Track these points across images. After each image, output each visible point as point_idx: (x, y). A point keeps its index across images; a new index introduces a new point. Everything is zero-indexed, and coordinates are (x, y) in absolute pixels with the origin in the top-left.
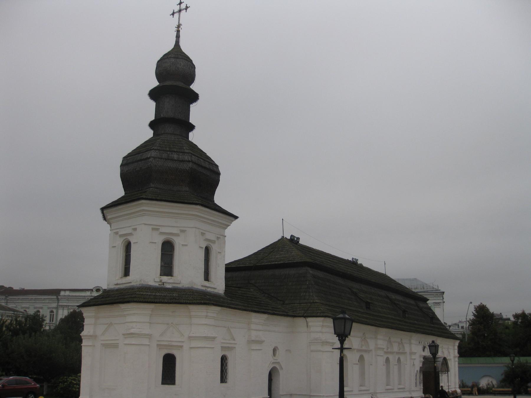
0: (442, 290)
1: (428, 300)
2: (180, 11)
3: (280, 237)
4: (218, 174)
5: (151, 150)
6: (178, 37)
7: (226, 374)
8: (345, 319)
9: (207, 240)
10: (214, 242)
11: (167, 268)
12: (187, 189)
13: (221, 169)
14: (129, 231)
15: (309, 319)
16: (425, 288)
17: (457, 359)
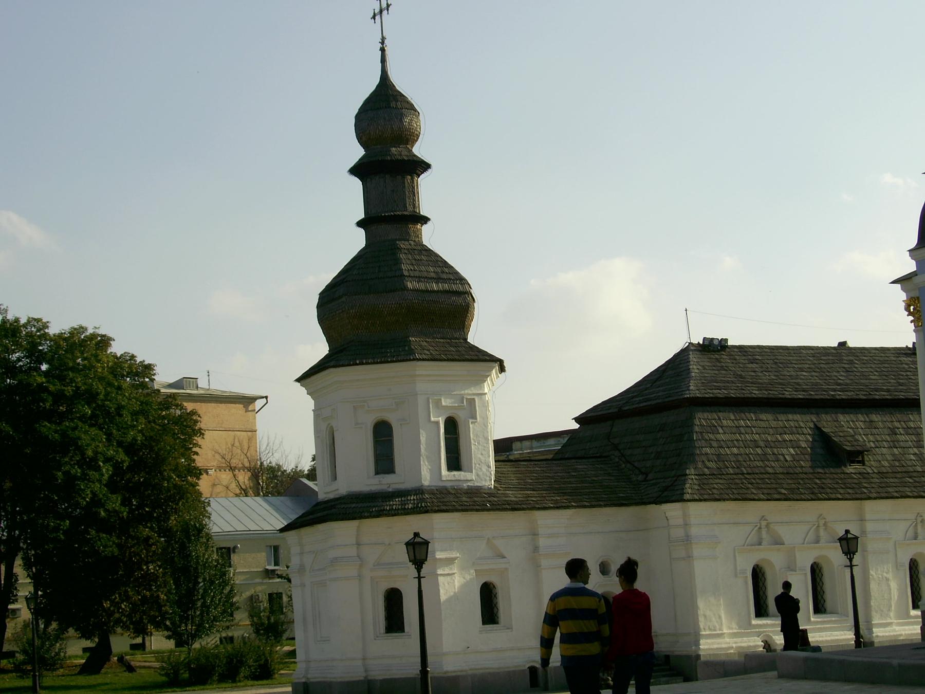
2: (381, 11)
6: (383, 60)
7: (495, 610)
11: (384, 460)
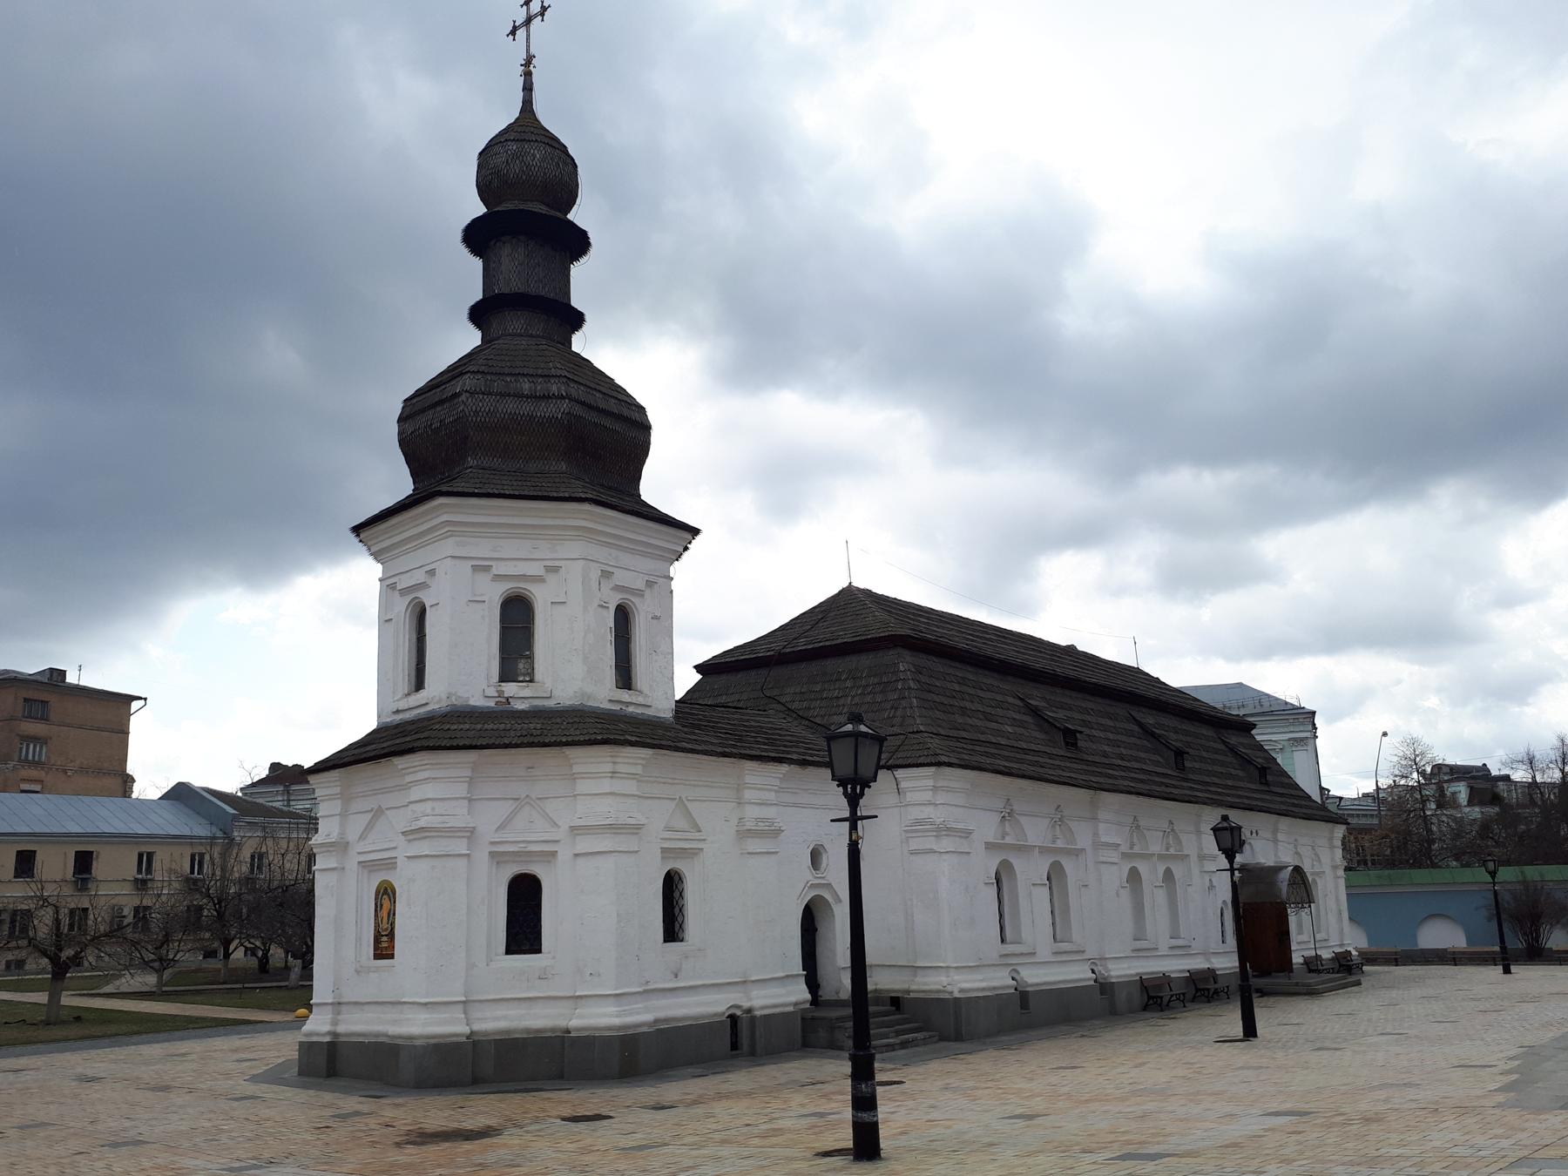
0: (1309, 706)
1: (1254, 726)
3: (846, 585)
4: (646, 428)
5: (462, 374)
8: (856, 735)
9: (618, 588)
10: (640, 593)
12: (563, 466)
13: (652, 417)
14: (419, 576)
15: (900, 773)
16: (1266, 704)
17: (1341, 872)
